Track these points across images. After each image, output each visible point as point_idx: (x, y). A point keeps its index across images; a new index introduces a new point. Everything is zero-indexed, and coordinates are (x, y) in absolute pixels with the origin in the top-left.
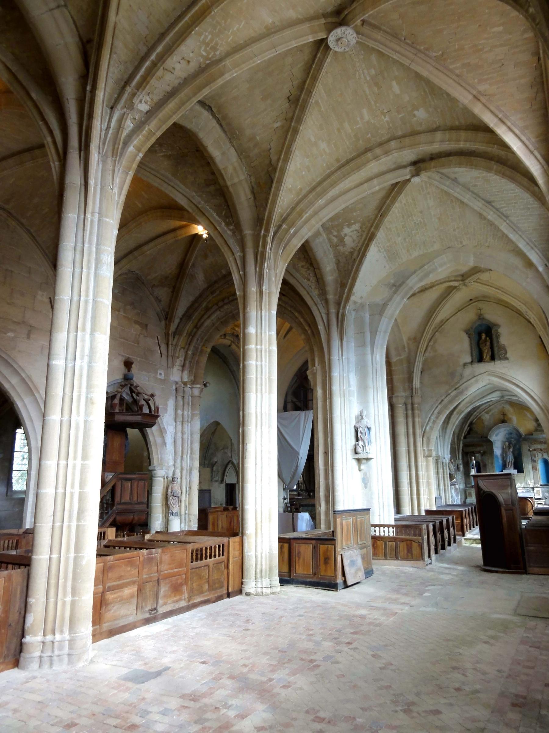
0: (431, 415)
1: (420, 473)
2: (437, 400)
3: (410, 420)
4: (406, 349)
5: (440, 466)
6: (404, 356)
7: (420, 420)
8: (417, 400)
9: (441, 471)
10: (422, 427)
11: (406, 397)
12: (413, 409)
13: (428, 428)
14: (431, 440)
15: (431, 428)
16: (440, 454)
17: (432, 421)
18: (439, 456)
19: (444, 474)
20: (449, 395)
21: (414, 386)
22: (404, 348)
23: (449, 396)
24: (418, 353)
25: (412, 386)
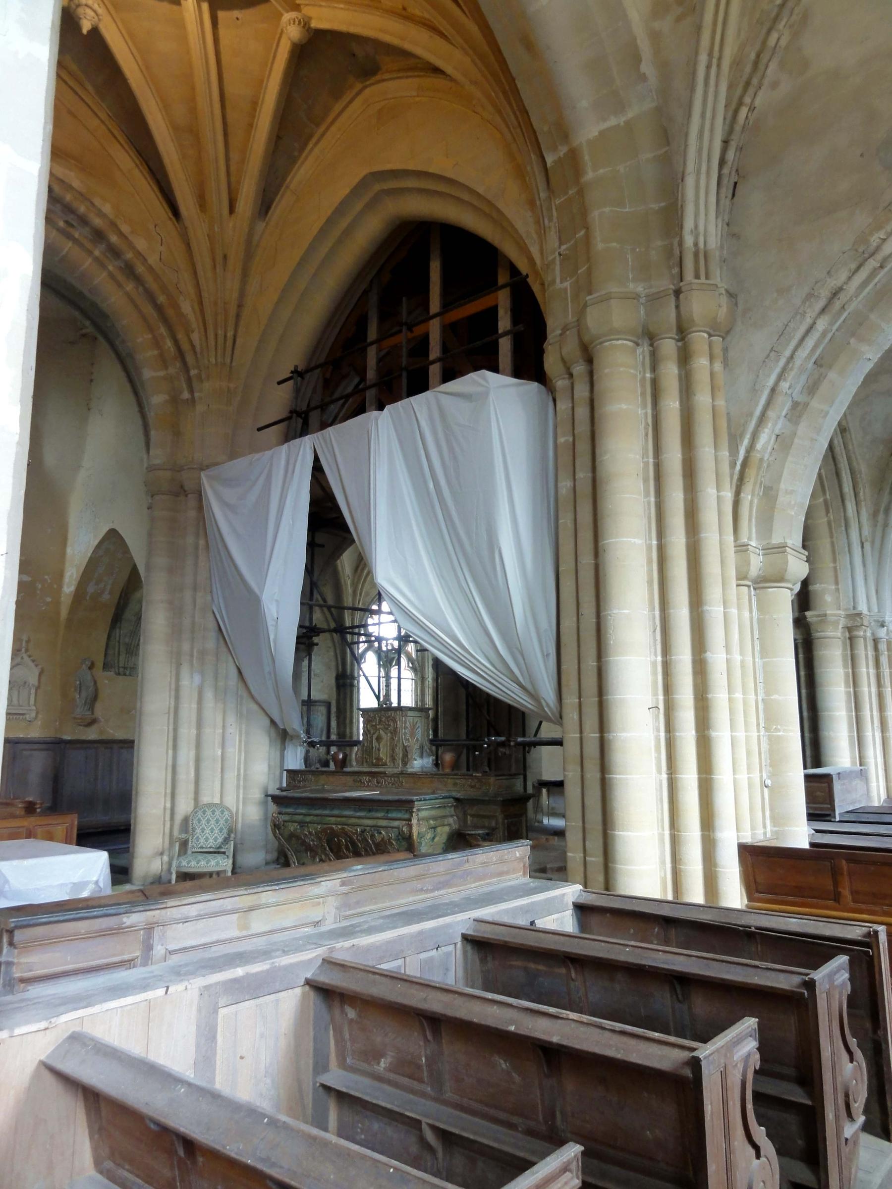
0: (780, 377)
1: (717, 658)
2: (810, 296)
3: (672, 405)
4: (647, 68)
5: (864, 652)
6: (639, 107)
7: (721, 403)
8: (703, 305)
9: (866, 671)
10: (734, 442)
11: (654, 299)
12: (685, 358)
13: (765, 439)
14: (782, 499)
15: (784, 443)
16: (863, 607)
17: (783, 406)
18: (859, 615)
19: (879, 685)
20: (872, 255)
21: (689, 241)
22: (637, 59)
23: (872, 263)
24: (703, 58)
25: (681, 244)
